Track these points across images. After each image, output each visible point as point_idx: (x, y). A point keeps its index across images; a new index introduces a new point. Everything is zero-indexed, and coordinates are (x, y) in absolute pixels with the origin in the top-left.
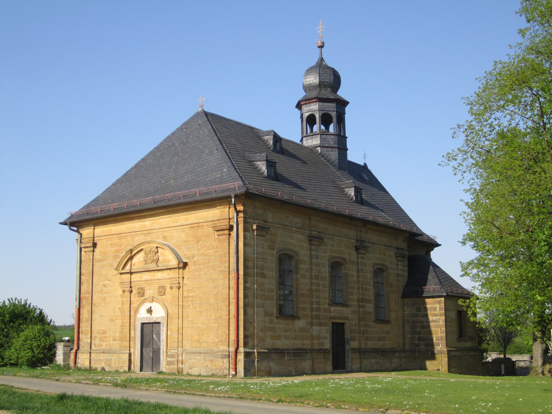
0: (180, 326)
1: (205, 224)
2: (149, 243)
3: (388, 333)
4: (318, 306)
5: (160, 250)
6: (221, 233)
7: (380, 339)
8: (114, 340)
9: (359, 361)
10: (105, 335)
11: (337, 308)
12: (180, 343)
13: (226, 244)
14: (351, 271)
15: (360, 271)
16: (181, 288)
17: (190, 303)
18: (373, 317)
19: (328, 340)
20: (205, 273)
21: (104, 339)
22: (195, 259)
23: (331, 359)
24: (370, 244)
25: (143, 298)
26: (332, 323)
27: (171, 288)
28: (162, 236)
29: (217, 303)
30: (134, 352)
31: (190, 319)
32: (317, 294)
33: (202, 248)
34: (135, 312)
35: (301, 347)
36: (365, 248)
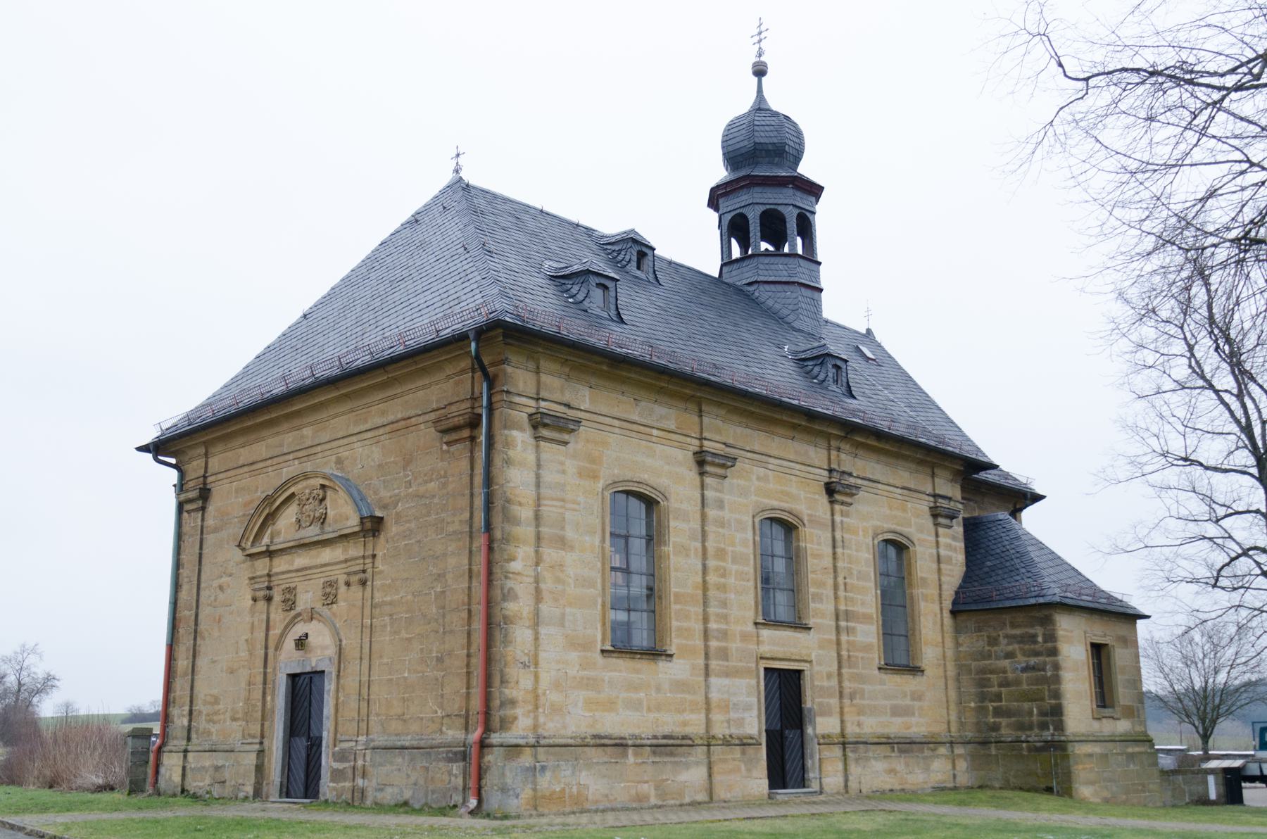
0: (365, 678)
1: (421, 419)
2: (305, 476)
3: (917, 697)
4: (723, 626)
5: (329, 493)
6: (454, 436)
7: (896, 711)
8: (234, 719)
9: (840, 766)
10: (217, 707)
11: (777, 633)
12: (363, 722)
13: (465, 464)
14: (814, 542)
15: (839, 544)
16: (369, 583)
17: (387, 619)
18: (876, 657)
19: (755, 713)
20: (419, 541)
21: (215, 718)
22: (400, 507)
23: (764, 763)
24: (865, 483)
25: (293, 613)
26: (766, 669)
27: (348, 584)
28: (334, 458)
29: (444, 616)
30: (270, 748)
31: (385, 660)
32: (723, 596)
33: (416, 479)
34: (276, 649)
35: (679, 731)
36: (851, 491)
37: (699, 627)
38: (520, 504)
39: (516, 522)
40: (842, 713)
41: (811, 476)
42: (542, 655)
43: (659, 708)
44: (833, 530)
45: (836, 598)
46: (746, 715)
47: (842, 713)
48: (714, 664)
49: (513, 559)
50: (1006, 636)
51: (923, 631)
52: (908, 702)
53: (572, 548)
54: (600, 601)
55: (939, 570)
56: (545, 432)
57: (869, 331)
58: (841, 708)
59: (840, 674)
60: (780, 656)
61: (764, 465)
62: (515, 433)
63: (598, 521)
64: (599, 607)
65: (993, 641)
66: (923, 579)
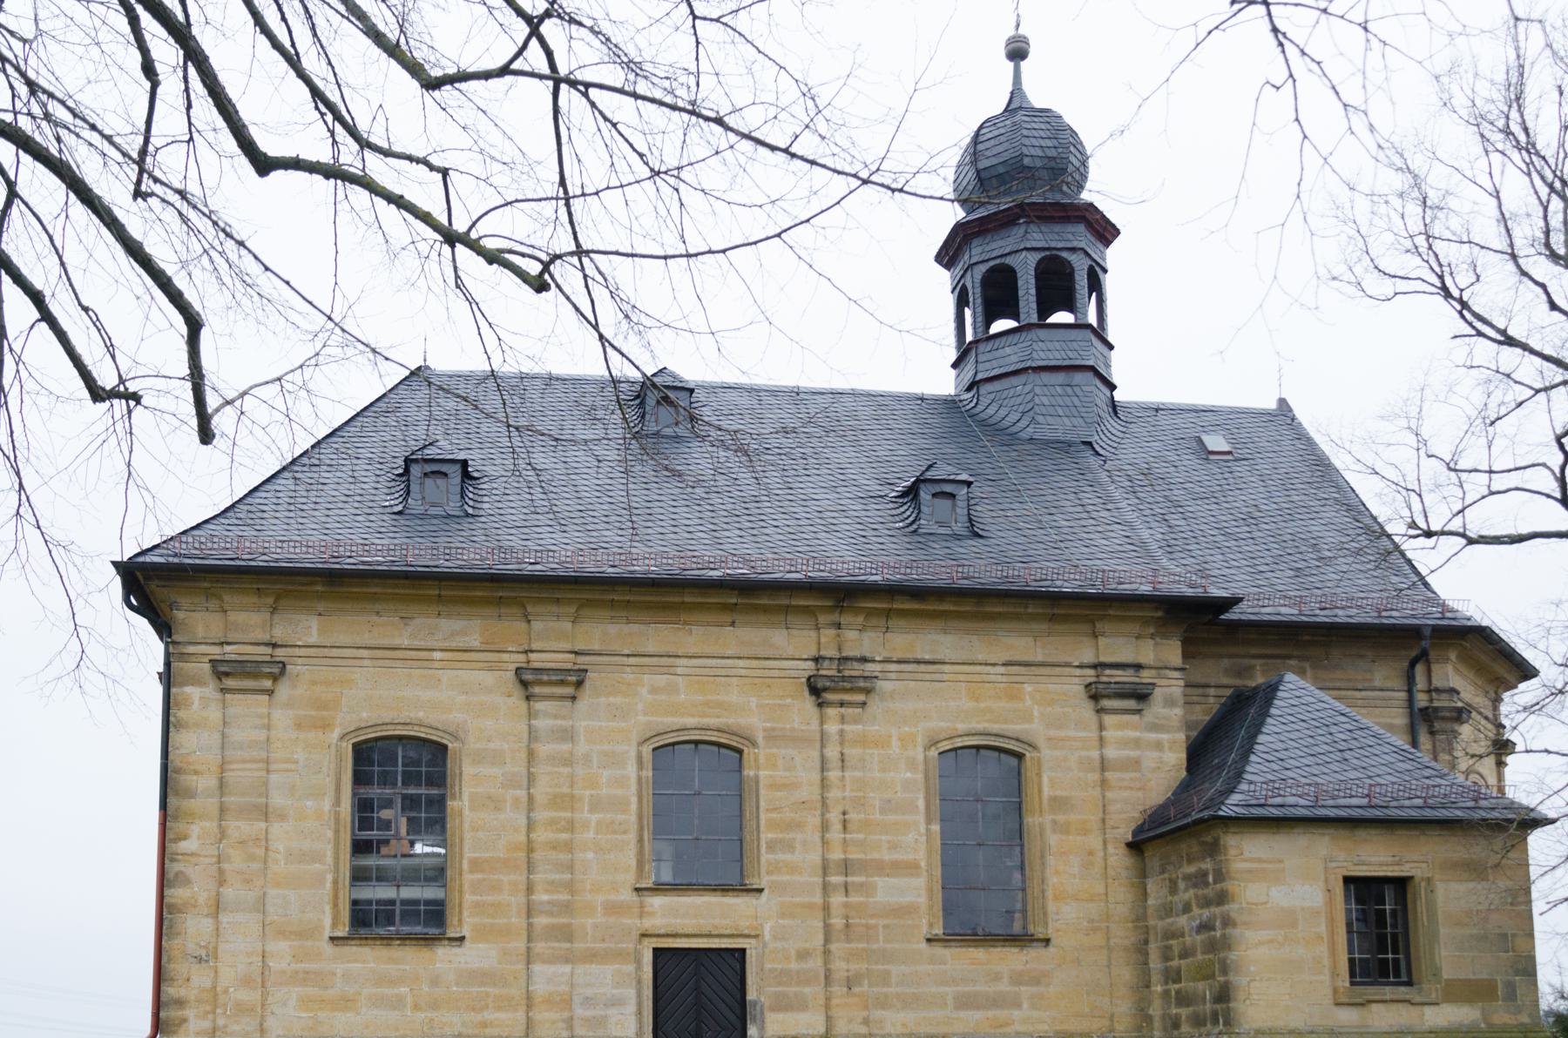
19: (631, 1008)
26: (655, 950)
37: (517, 900)
40: (827, 1007)
41: (776, 673)
42: (222, 947)
43: (435, 1005)
44: (823, 746)
45: (825, 842)
46: (611, 1012)
47: (827, 1007)
48: (539, 947)
51: (1053, 880)
52: (1004, 987)
53: (282, 817)
54: (330, 878)
55: (1104, 783)
56: (230, 683)
57: (1282, 402)
58: (828, 999)
59: (827, 952)
60: (690, 931)
61: (669, 671)
62: (188, 689)
63: (329, 783)
64: (329, 885)
65: (1173, 889)
66: (1059, 803)
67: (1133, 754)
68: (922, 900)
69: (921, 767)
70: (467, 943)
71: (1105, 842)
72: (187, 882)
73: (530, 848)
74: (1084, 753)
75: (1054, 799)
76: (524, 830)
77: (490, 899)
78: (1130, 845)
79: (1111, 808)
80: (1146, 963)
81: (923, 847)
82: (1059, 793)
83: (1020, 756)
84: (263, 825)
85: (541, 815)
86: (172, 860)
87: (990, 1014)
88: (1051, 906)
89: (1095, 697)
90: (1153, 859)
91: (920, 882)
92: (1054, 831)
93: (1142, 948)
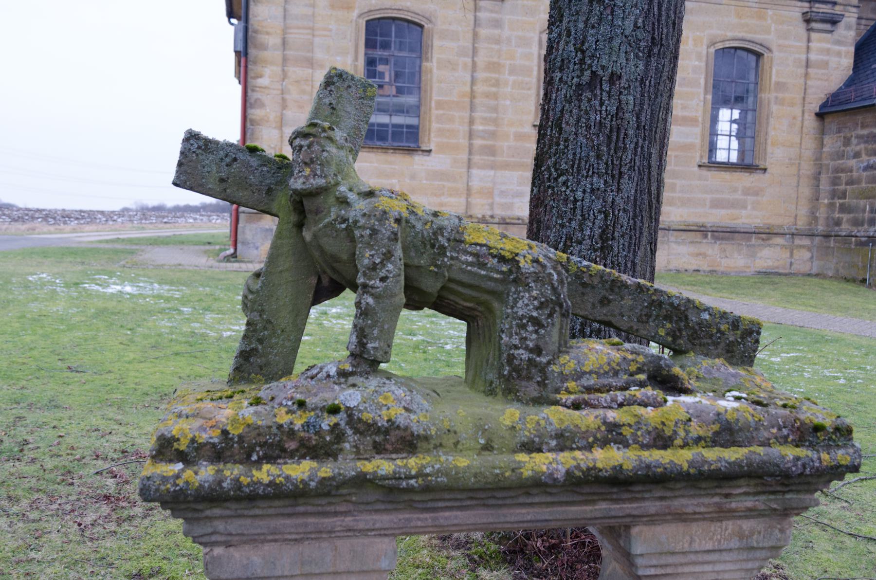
7: (717, 204)
37: (464, 128)
38: (268, 33)
39: (263, 47)
46: (516, 200)
48: (476, 158)
49: (261, 76)
50: (858, 137)
51: (772, 133)
52: (738, 196)
55: (806, 75)
63: (351, 46)
65: (847, 142)
66: (781, 86)
67: (825, 58)
68: (698, 141)
69: (704, 59)
70: (433, 154)
71: (803, 112)
72: (262, 105)
73: (473, 96)
74: (797, 56)
75: (777, 83)
76: (469, 84)
77: (447, 126)
78: (817, 115)
79: (809, 91)
80: (818, 186)
81: (701, 109)
82: (781, 80)
83: (758, 55)
84: (310, 71)
85: (480, 75)
86: (253, 91)
87: (729, 212)
88: (769, 149)
89: (808, 21)
90: (832, 123)
91: (698, 130)
92: (776, 103)
93: (817, 177)
